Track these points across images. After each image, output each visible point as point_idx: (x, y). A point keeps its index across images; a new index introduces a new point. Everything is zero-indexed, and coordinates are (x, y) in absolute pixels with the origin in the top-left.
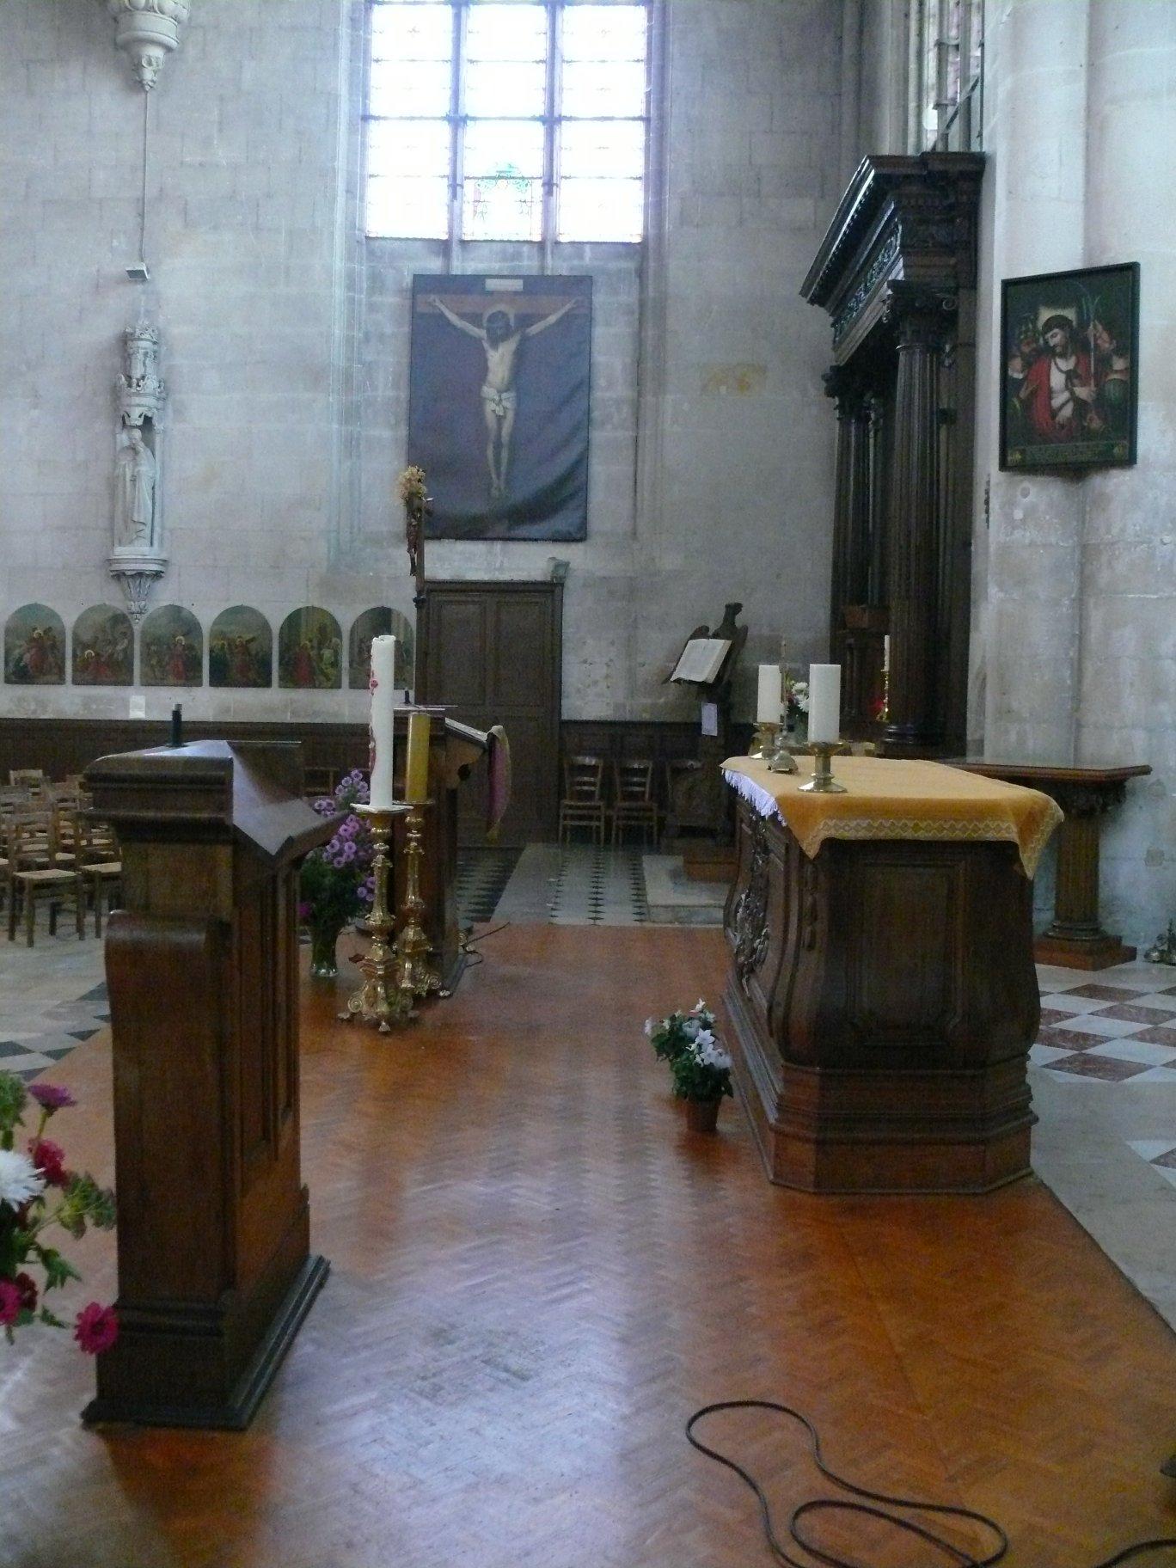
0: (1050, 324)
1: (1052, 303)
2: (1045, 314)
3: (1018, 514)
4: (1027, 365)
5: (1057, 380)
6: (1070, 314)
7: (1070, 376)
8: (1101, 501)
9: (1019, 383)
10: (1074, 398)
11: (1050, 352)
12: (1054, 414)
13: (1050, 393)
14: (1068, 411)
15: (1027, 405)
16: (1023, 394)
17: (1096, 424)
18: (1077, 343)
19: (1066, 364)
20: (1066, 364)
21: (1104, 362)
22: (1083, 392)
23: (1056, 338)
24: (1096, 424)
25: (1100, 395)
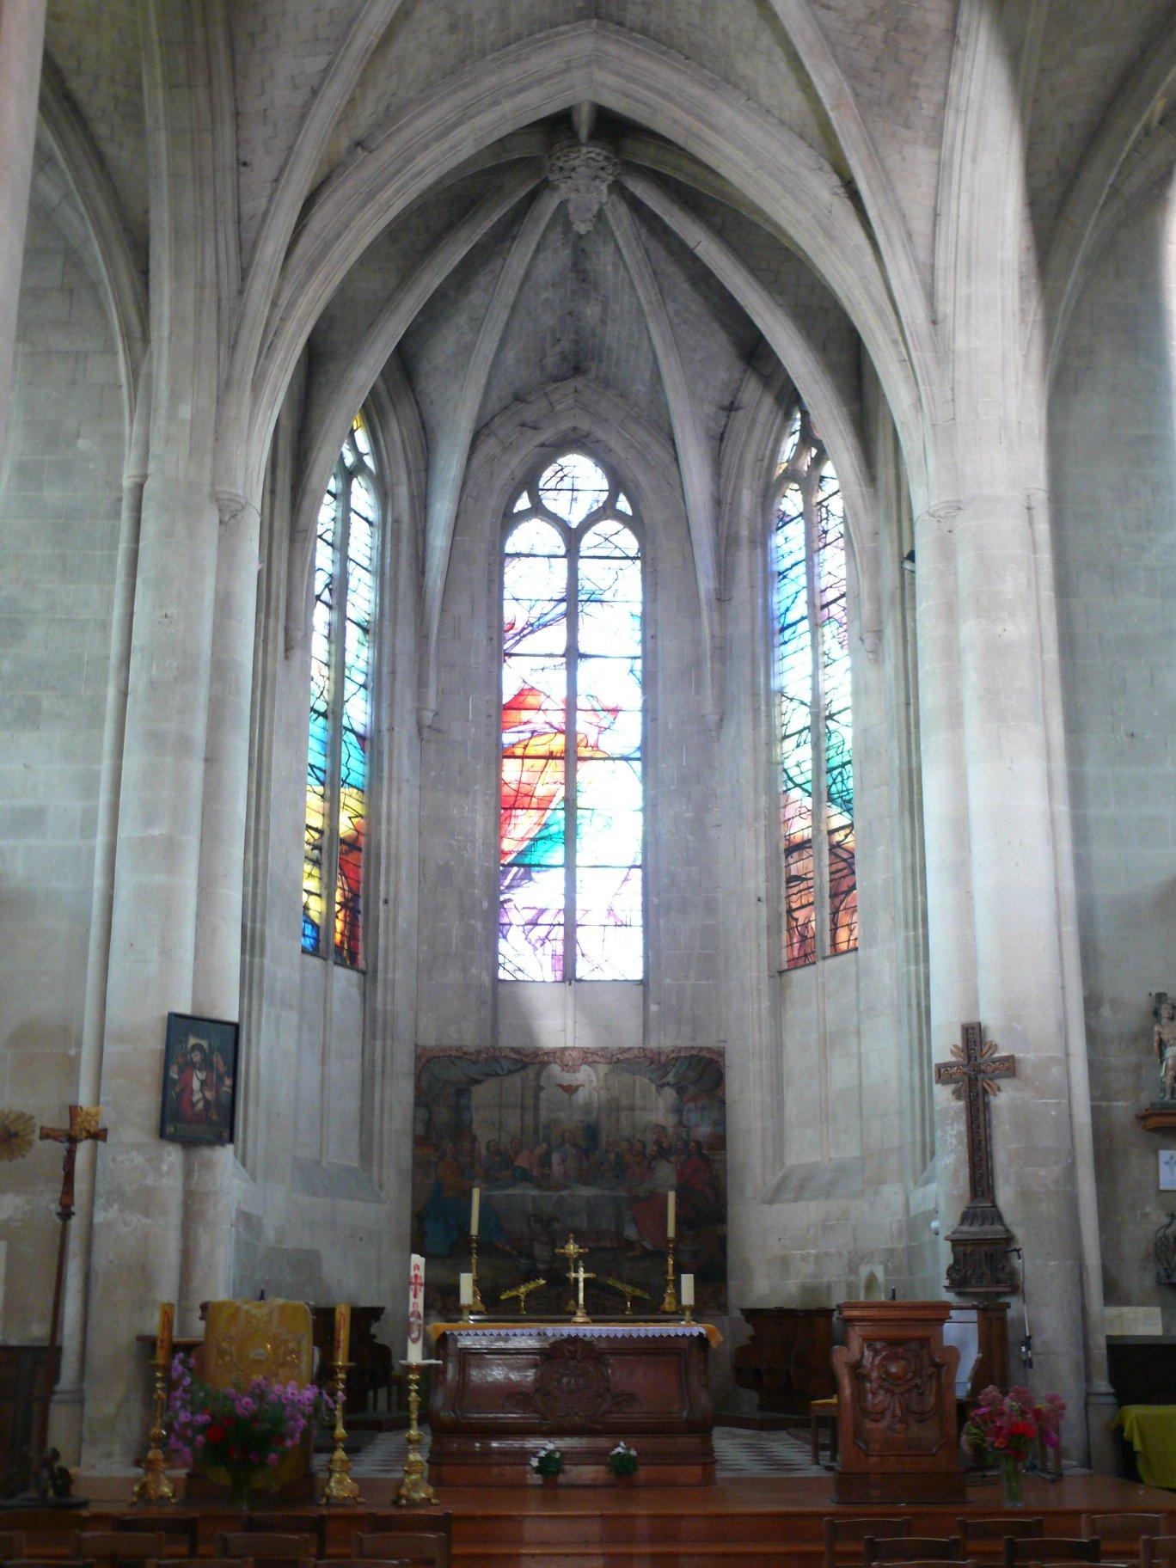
0: (194, 1047)
1: (198, 1036)
2: (192, 1041)
3: (165, 1168)
4: (180, 1072)
5: (196, 1084)
6: (205, 1043)
7: (203, 1083)
8: (208, 1165)
9: (175, 1082)
10: (204, 1098)
11: (191, 1065)
12: (194, 1105)
13: (192, 1093)
14: (200, 1106)
15: (179, 1095)
16: (178, 1089)
17: (215, 1117)
18: (207, 1064)
19: (202, 1075)
20: (202, 1075)
21: (220, 1078)
22: (209, 1095)
23: (197, 1057)
24: (215, 1117)
25: (218, 1101)
